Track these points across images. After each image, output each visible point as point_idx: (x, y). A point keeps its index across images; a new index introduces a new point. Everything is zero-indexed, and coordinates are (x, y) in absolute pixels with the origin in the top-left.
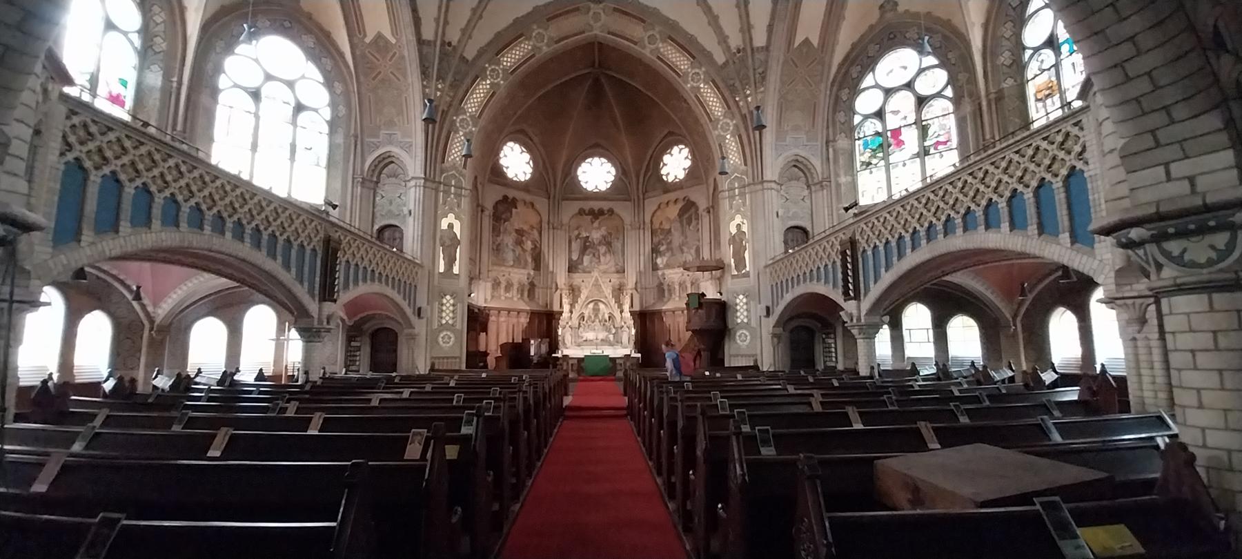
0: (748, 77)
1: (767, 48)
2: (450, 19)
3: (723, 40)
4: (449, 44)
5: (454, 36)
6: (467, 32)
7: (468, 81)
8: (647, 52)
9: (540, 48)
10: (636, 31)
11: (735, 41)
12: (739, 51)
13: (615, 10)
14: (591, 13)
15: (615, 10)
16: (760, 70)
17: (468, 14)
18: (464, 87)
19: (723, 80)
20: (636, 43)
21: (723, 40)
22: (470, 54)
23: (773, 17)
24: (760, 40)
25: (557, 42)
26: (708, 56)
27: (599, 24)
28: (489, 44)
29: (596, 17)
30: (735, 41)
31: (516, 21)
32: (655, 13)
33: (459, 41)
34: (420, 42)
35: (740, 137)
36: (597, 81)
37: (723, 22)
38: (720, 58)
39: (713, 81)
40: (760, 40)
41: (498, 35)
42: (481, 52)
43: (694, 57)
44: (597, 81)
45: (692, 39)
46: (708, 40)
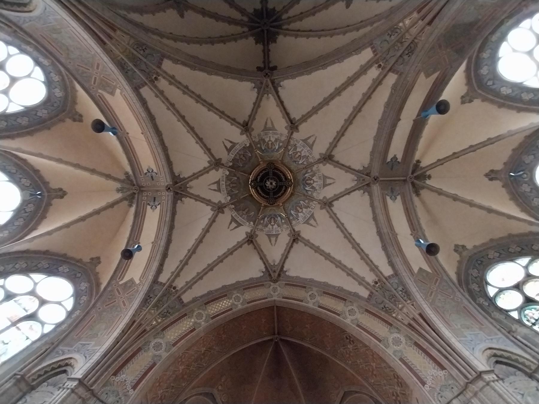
0: (394, 296)
1: (396, 274)
2: (181, 274)
3: (361, 281)
4: (174, 288)
5: (180, 283)
6: (189, 285)
7: (177, 315)
8: (310, 305)
9: (237, 306)
10: (300, 293)
11: (370, 278)
12: (376, 283)
13: (286, 284)
14: (271, 287)
15: (286, 284)
16: (400, 289)
17: (194, 274)
18: (172, 318)
19: (374, 305)
20: (302, 301)
21: (361, 281)
22: (186, 298)
23: (388, 256)
24: (387, 271)
25: (248, 303)
26: (356, 295)
27: (276, 293)
28: (201, 297)
29: (275, 290)
30: (370, 278)
31: (224, 287)
32: (312, 281)
33: (182, 288)
34: (155, 281)
35: (417, 344)
36: (277, 351)
37: (356, 270)
38: (364, 293)
39: (367, 311)
40: (387, 271)
41: (210, 293)
42: (195, 300)
43: (345, 300)
44: (277, 351)
45: (341, 289)
46: (350, 285)
